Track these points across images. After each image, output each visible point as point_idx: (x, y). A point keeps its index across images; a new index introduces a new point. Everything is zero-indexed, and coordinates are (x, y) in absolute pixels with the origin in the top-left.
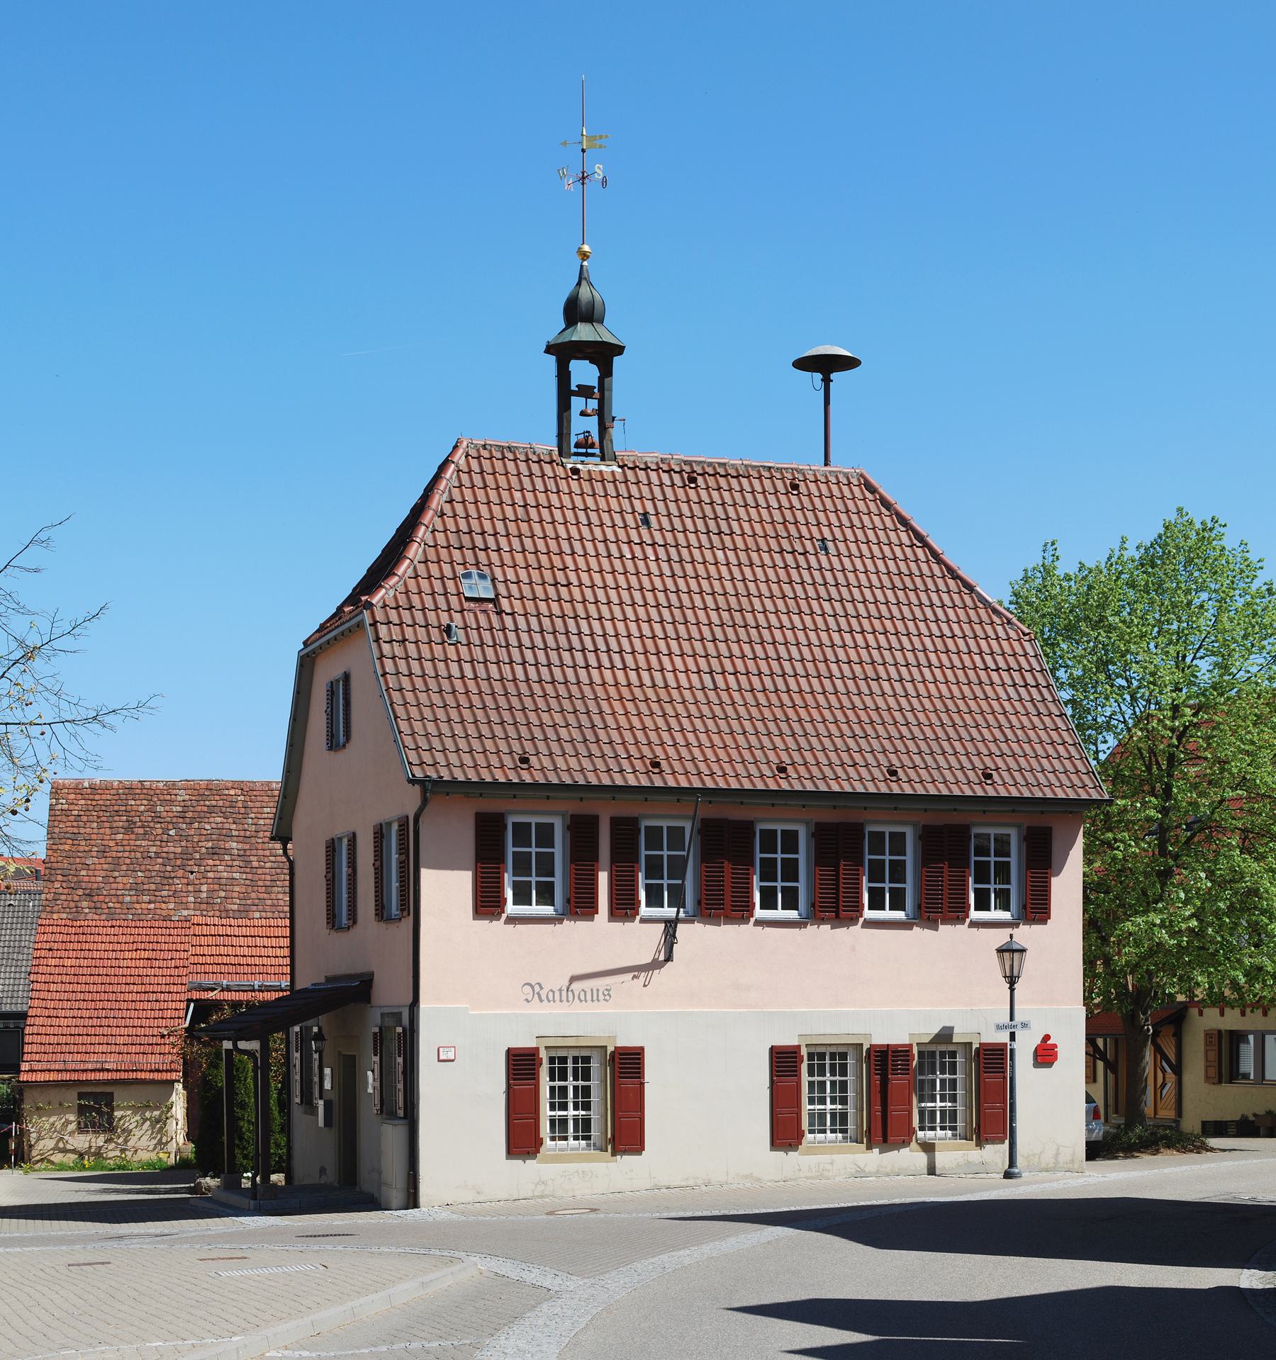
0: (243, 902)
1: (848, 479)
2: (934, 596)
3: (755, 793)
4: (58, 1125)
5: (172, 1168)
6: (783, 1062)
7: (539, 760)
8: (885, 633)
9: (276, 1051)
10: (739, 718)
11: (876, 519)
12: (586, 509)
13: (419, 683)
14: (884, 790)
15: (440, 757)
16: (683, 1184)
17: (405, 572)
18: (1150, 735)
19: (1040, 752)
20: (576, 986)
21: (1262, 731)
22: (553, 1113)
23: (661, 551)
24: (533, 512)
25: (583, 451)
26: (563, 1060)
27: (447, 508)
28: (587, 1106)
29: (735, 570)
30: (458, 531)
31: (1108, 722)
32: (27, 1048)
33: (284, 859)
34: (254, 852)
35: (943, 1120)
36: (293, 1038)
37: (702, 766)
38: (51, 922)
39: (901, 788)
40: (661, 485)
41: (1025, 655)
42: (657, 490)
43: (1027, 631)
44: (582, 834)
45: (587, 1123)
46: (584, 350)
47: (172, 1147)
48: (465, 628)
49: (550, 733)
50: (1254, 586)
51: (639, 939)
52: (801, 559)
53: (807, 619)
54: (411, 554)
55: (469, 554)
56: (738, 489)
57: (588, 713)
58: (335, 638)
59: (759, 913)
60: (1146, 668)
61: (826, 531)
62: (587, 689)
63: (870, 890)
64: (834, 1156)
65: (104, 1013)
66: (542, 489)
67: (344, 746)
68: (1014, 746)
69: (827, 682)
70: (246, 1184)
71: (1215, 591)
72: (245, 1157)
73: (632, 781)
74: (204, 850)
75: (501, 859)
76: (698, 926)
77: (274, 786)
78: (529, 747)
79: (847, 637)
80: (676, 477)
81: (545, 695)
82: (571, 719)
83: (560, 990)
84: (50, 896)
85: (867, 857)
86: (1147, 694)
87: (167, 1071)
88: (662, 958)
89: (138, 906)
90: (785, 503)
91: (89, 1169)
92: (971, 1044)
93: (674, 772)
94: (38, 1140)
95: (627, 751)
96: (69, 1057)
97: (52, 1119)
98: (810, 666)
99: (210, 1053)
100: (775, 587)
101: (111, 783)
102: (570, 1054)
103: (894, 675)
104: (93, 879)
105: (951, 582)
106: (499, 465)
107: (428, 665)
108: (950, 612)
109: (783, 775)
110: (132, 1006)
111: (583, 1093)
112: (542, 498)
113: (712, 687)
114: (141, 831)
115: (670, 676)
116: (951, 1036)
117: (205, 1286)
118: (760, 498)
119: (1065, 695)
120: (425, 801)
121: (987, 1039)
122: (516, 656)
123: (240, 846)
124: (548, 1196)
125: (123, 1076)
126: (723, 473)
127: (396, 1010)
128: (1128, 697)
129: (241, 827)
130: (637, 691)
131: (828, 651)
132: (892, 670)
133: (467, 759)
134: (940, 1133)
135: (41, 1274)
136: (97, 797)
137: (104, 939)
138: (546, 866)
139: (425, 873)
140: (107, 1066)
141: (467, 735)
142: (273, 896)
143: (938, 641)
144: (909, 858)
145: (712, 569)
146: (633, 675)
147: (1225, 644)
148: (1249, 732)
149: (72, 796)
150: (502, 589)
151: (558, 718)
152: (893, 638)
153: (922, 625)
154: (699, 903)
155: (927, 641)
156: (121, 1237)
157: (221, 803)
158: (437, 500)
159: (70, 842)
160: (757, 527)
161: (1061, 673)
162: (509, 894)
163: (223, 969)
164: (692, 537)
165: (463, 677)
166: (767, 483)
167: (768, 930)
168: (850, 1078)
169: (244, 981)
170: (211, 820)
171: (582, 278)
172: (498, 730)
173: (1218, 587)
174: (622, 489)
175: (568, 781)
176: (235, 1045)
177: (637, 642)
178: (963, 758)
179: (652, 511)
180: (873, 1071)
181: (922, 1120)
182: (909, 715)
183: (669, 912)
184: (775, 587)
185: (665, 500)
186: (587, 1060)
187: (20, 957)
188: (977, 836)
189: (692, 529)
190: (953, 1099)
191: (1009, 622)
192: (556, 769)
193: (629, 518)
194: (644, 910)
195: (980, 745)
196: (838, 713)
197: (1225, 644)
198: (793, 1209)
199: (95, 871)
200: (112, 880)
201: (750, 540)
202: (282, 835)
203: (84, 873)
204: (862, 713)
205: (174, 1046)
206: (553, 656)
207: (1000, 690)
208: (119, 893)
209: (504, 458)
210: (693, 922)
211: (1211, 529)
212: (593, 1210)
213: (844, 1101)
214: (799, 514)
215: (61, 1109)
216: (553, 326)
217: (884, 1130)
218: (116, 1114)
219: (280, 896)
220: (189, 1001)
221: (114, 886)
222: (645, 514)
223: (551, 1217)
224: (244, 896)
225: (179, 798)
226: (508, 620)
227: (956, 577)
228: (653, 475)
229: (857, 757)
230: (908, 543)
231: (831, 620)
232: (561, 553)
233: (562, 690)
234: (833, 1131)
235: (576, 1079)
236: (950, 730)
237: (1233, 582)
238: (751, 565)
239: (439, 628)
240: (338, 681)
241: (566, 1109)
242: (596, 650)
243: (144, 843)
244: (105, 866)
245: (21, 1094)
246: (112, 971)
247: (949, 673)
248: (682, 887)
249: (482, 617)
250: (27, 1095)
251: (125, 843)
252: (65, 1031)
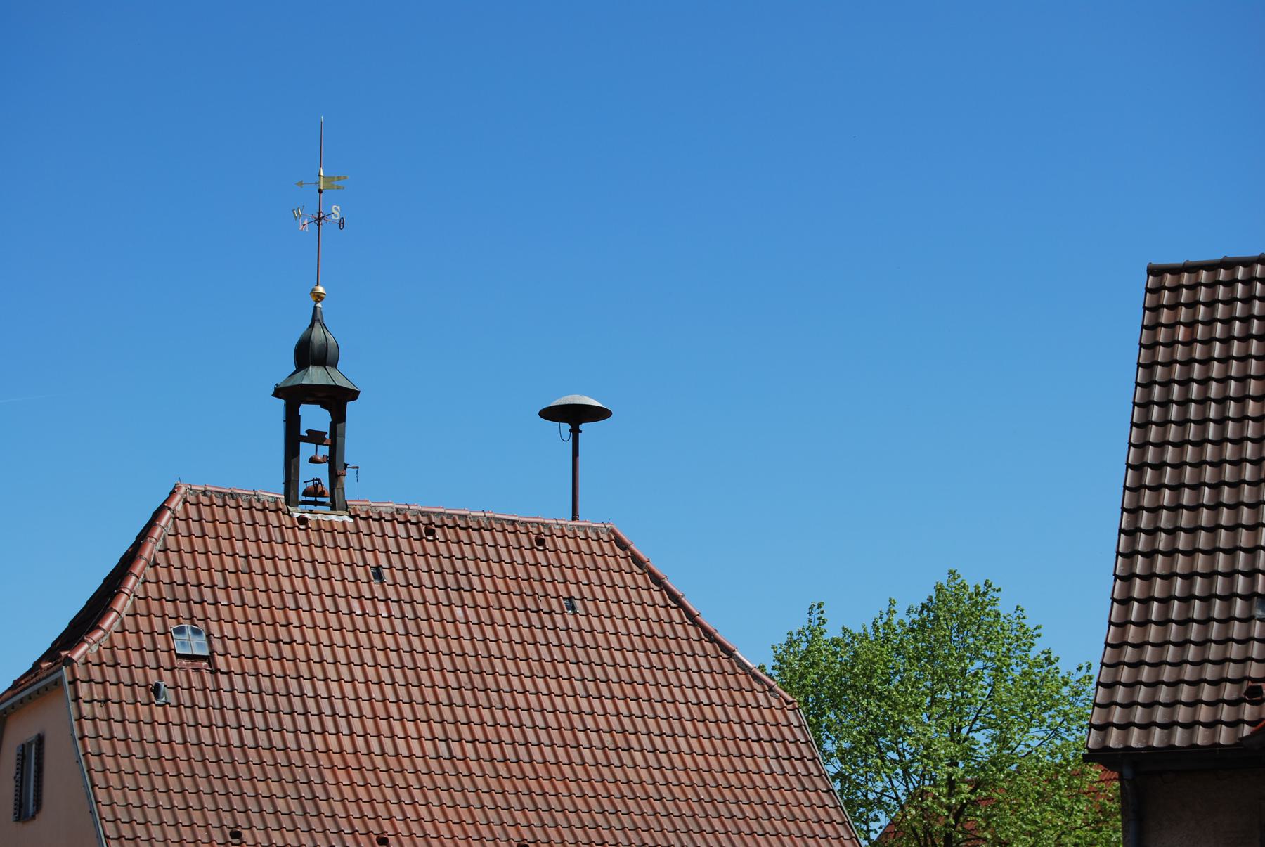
1: (597, 534)
2: (690, 660)
8: (637, 699)
10: (476, 791)
11: (628, 577)
12: (313, 561)
13: (121, 748)
17: (111, 625)
18: (925, 812)
19: (806, 831)
21: (1045, 810)
23: (394, 607)
24: (255, 564)
25: (312, 499)
27: (161, 558)
29: (475, 629)
30: (172, 582)
31: (879, 800)
40: (396, 537)
41: (789, 725)
42: (391, 542)
43: (790, 699)
46: (315, 394)
48: (176, 687)
49: (267, 806)
50: (1032, 655)
52: (546, 618)
53: (553, 683)
54: (118, 607)
55: (183, 608)
56: (479, 542)
57: (309, 782)
58: (30, 697)
60: (918, 740)
61: (573, 588)
62: (309, 757)
66: (266, 539)
67: (34, 817)
68: (778, 824)
69: (573, 752)
71: (991, 659)
78: (241, 819)
79: (596, 703)
80: (413, 529)
81: (262, 763)
82: (290, 789)
86: (921, 769)
90: (530, 559)
95: (352, 826)
98: (555, 734)
100: (518, 648)
103: (647, 745)
105: (708, 646)
106: (219, 513)
107: (132, 729)
108: (708, 677)
112: (265, 548)
113: (447, 756)
115: (401, 744)
118: (504, 552)
119: (831, 769)
122: (231, 720)
126: (463, 525)
128: (900, 771)
130: (365, 760)
131: (576, 718)
132: (645, 739)
141: (173, 807)
143: (694, 709)
145: (450, 627)
146: (360, 742)
147: (1003, 716)
148: (1031, 812)
150: (218, 646)
152: (645, 705)
153: (677, 691)
155: (683, 708)
158: (151, 549)
160: (500, 583)
161: (828, 746)
164: (428, 593)
165: (170, 742)
166: (511, 537)
171: (315, 319)
172: (208, 802)
173: (992, 655)
174: (353, 540)
177: (366, 706)
179: (385, 565)
182: (663, 789)
184: (518, 648)
185: (400, 552)
189: (429, 585)
191: (771, 689)
193: (360, 572)
195: (741, 823)
196: (586, 787)
197: (1003, 716)
201: (492, 598)
204: (612, 787)
206: (272, 719)
207: (761, 762)
209: (225, 505)
211: (985, 594)
214: (544, 571)
216: (283, 368)
222: (378, 568)
226: (223, 680)
227: (713, 640)
228: (388, 526)
230: (662, 603)
231: (578, 685)
232: (284, 608)
233: (281, 757)
236: (708, 806)
237: (1009, 650)
238: (493, 623)
239: (146, 686)
240: (30, 744)
242: (320, 714)
247: (706, 743)
249: (195, 677)
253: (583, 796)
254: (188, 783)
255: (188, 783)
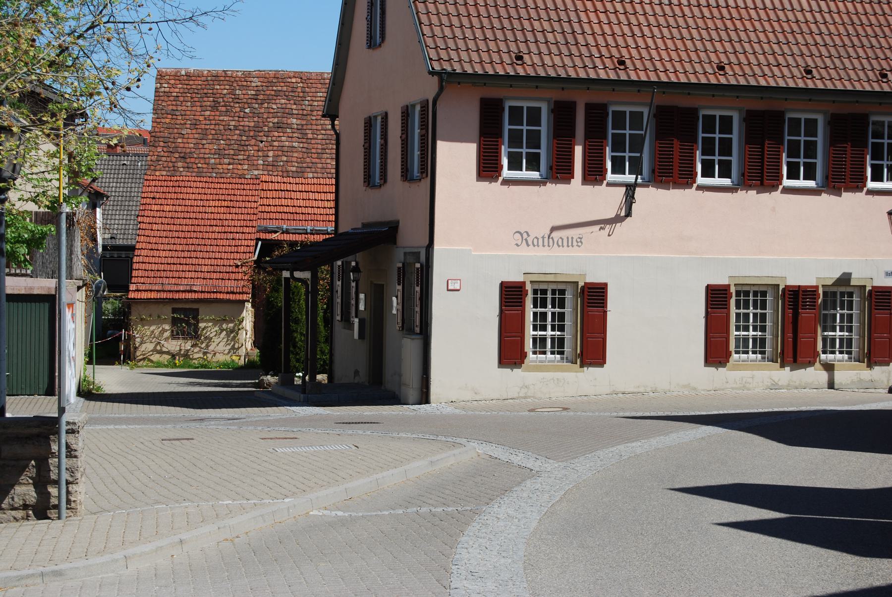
0: (300, 165)
3: (699, 86)
4: (157, 332)
5: (242, 367)
6: (716, 297)
7: (531, 58)
9: (323, 279)
14: (801, 85)
15: (453, 55)
16: (636, 390)
20: (556, 235)
22: (535, 333)
26: (544, 292)
28: (562, 328)
32: (135, 273)
33: (332, 132)
34: (309, 127)
35: (841, 346)
36: (336, 270)
37: (658, 65)
38: (155, 178)
39: (815, 84)
44: (563, 115)
45: (561, 341)
47: (242, 352)
49: (540, 37)
51: (605, 198)
57: (570, 21)
59: (700, 180)
63: (788, 164)
64: (755, 372)
65: (193, 248)
67: (380, 45)
70: (298, 381)
72: (298, 361)
73: (603, 75)
74: (271, 125)
75: (500, 135)
76: (652, 190)
77: (326, 76)
78: (523, 47)
82: (556, 26)
83: (543, 237)
84: (154, 158)
85: (787, 138)
87: (240, 293)
88: (623, 214)
89: (220, 167)
91: (181, 366)
92: (865, 286)
93: (636, 69)
94: (141, 343)
95: (600, 52)
96: (166, 281)
97: (152, 328)
99: (273, 280)
101: (202, 72)
102: (550, 287)
104: (186, 145)
109: (722, 73)
110: (214, 242)
111: (561, 318)
114: (224, 109)
116: (849, 280)
117: (265, 459)
120: (441, 89)
121: (877, 283)
123: (299, 122)
124: (530, 397)
125: (207, 296)
127: (416, 250)
129: (300, 107)
133: (475, 57)
134: (838, 356)
135: (142, 446)
136: (191, 83)
137: (195, 190)
138: (534, 140)
139: (441, 145)
140: (194, 288)
141: (475, 38)
142: (323, 161)
144: (820, 140)
149: (172, 82)
151: (546, 26)
154: (653, 171)
156: (202, 420)
157: (285, 89)
159: (170, 116)
162: (505, 162)
163: (284, 216)
167: (707, 194)
168: (768, 311)
169: (300, 226)
170: (278, 101)
172: (499, 35)
175: (553, 75)
176: (292, 274)
178: (864, 62)
180: (787, 306)
181: (824, 346)
183: (629, 178)
186: (562, 292)
187: (131, 203)
188: (874, 123)
190: (850, 330)
192: (543, 65)
194: (610, 177)
198: (721, 412)
199: (188, 139)
200: (201, 146)
202: (331, 113)
203: (180, 140)
204: (785, 25)
205: (245, 273)
208: (206, 156)
210: (648, 186)
212: (565, 409)
213: (763, 329)
215: (159, 320)
217: (795, 352)
218: (200, 325)
219: (329, 161)
220: (258, 240)
221: (203, 151)
223: (532, 413)
224: (301, 161)
225: (253, 84)
229: (780, 59)
234: (754, 352)
235: (553, 306)
236: (855, 39)
241: (545, 330)
243: (226, 118)
244: (196, 136)
245: (129, 308)
246: (200, 216)
248: (641, 157)
250: (134, 309)
251: (211, 118)
252: (164, 260)
253: (764, 31)
254: (486, 22)
255: (486, 22)
